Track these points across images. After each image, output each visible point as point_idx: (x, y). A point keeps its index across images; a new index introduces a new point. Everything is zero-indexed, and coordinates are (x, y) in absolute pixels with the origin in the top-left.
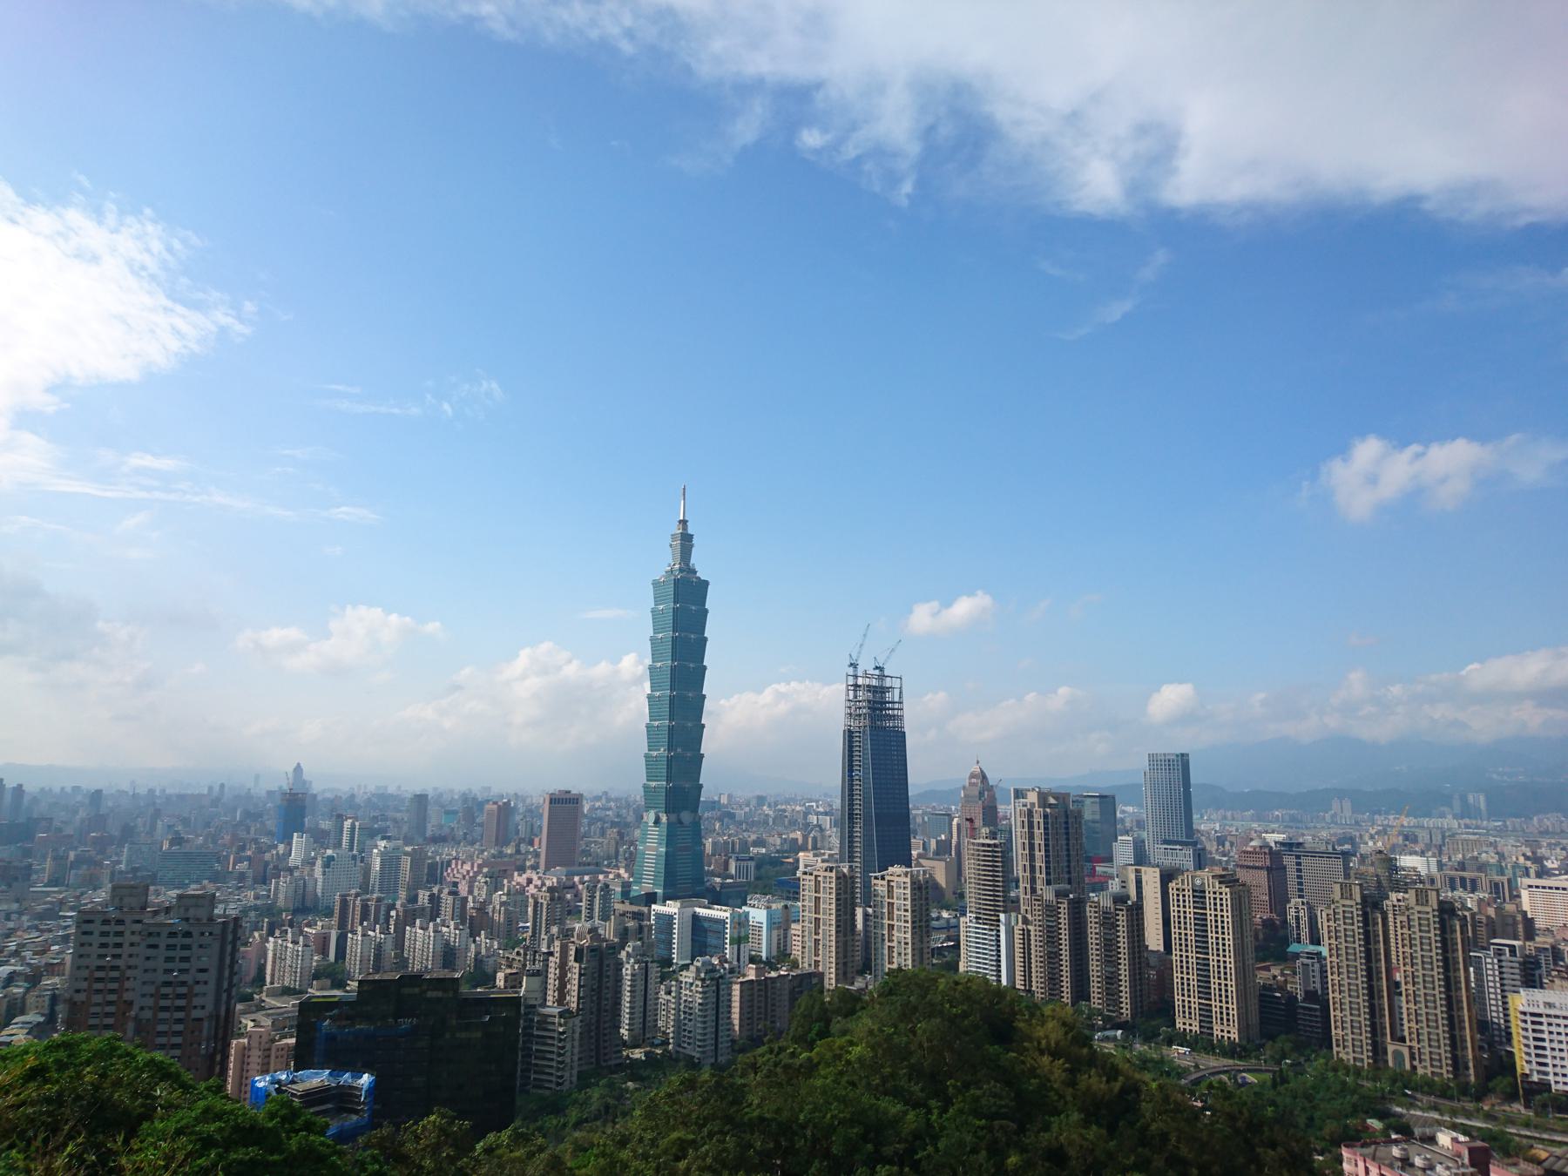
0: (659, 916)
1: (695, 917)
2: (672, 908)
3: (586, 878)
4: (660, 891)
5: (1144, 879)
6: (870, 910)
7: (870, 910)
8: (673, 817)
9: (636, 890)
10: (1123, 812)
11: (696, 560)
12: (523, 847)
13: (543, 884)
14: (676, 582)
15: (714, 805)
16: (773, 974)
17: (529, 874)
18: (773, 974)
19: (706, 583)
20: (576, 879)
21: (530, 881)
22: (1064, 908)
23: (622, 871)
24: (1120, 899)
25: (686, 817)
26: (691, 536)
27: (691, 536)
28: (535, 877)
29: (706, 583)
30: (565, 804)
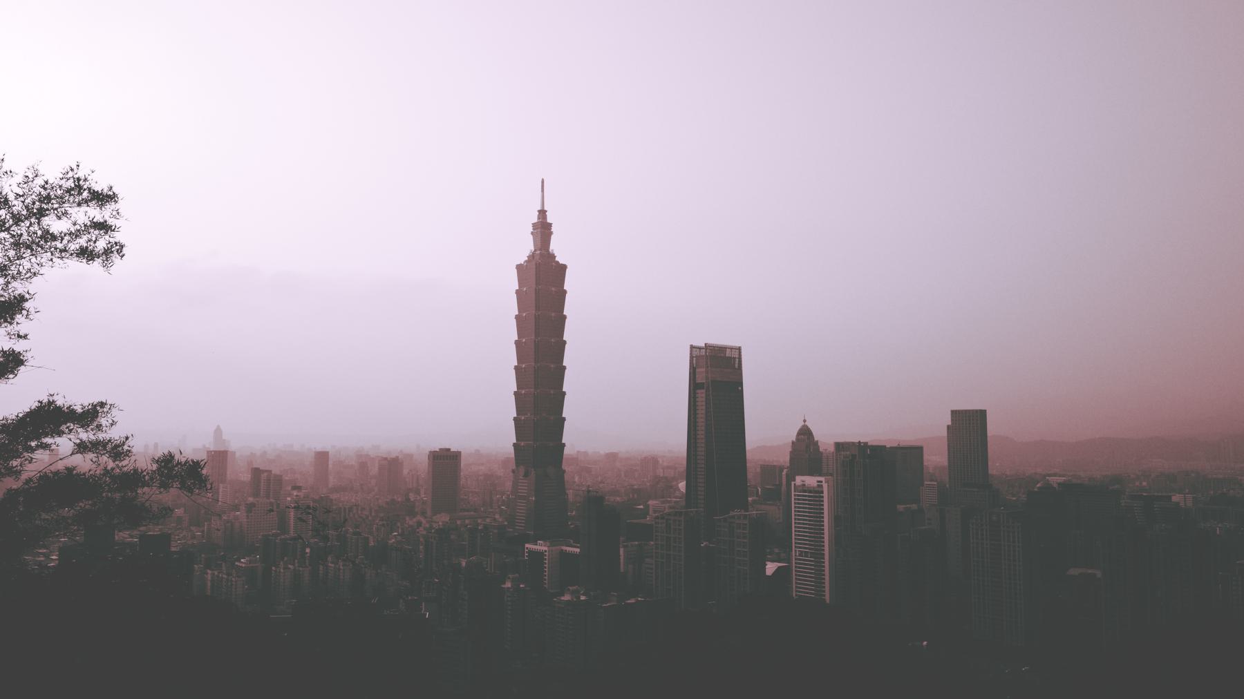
0: (531, 552)
2: (541, 547)
11: (555, 246)
12: (412, 497)
13: (431, 527)
14: (538, 266)
15: (574, 460)
16: (632, 601)
17: (419, 518)
18: (632, 601)
19: (564, 267)
21: (419, 524)
23: (497, 516)
26: (550, 225)
27: (550, 225)
28: (424, 521)
29: (564, 267)
30: (445, 461)
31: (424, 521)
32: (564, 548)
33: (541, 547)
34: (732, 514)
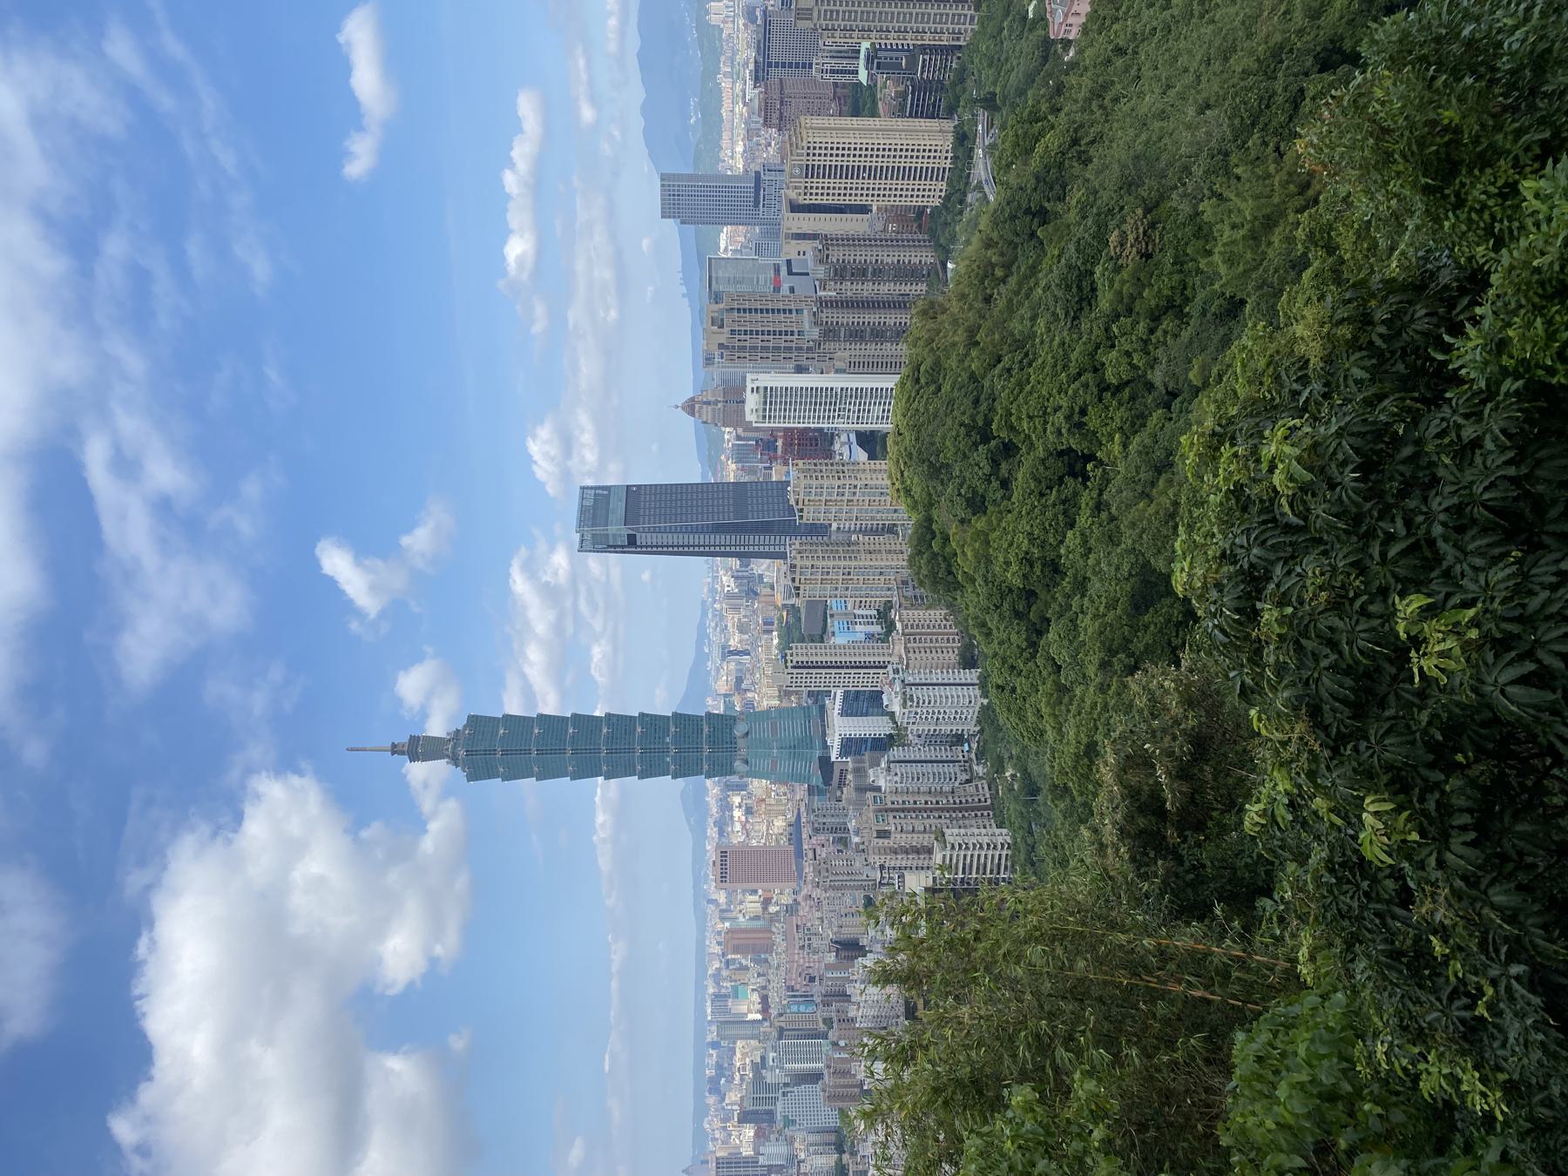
1: (844, 713)
2: (834, 743)
3: (804, 836)
4: (818, 753)
5: (795, 231)
6: (834, 526)
7: (834, 526)
8: (741, 743)
9: (817, 780)
10: (726, 250)
17: (800, 899)
18: (899, 625)
20: (805, 847)
22: (829, 316)
24: (823, 260)
25: (740, 729)
28: (804, 892)
31: (804, 892)
32: (836, 711)
33: (834, 743)
34: (792, 502)
